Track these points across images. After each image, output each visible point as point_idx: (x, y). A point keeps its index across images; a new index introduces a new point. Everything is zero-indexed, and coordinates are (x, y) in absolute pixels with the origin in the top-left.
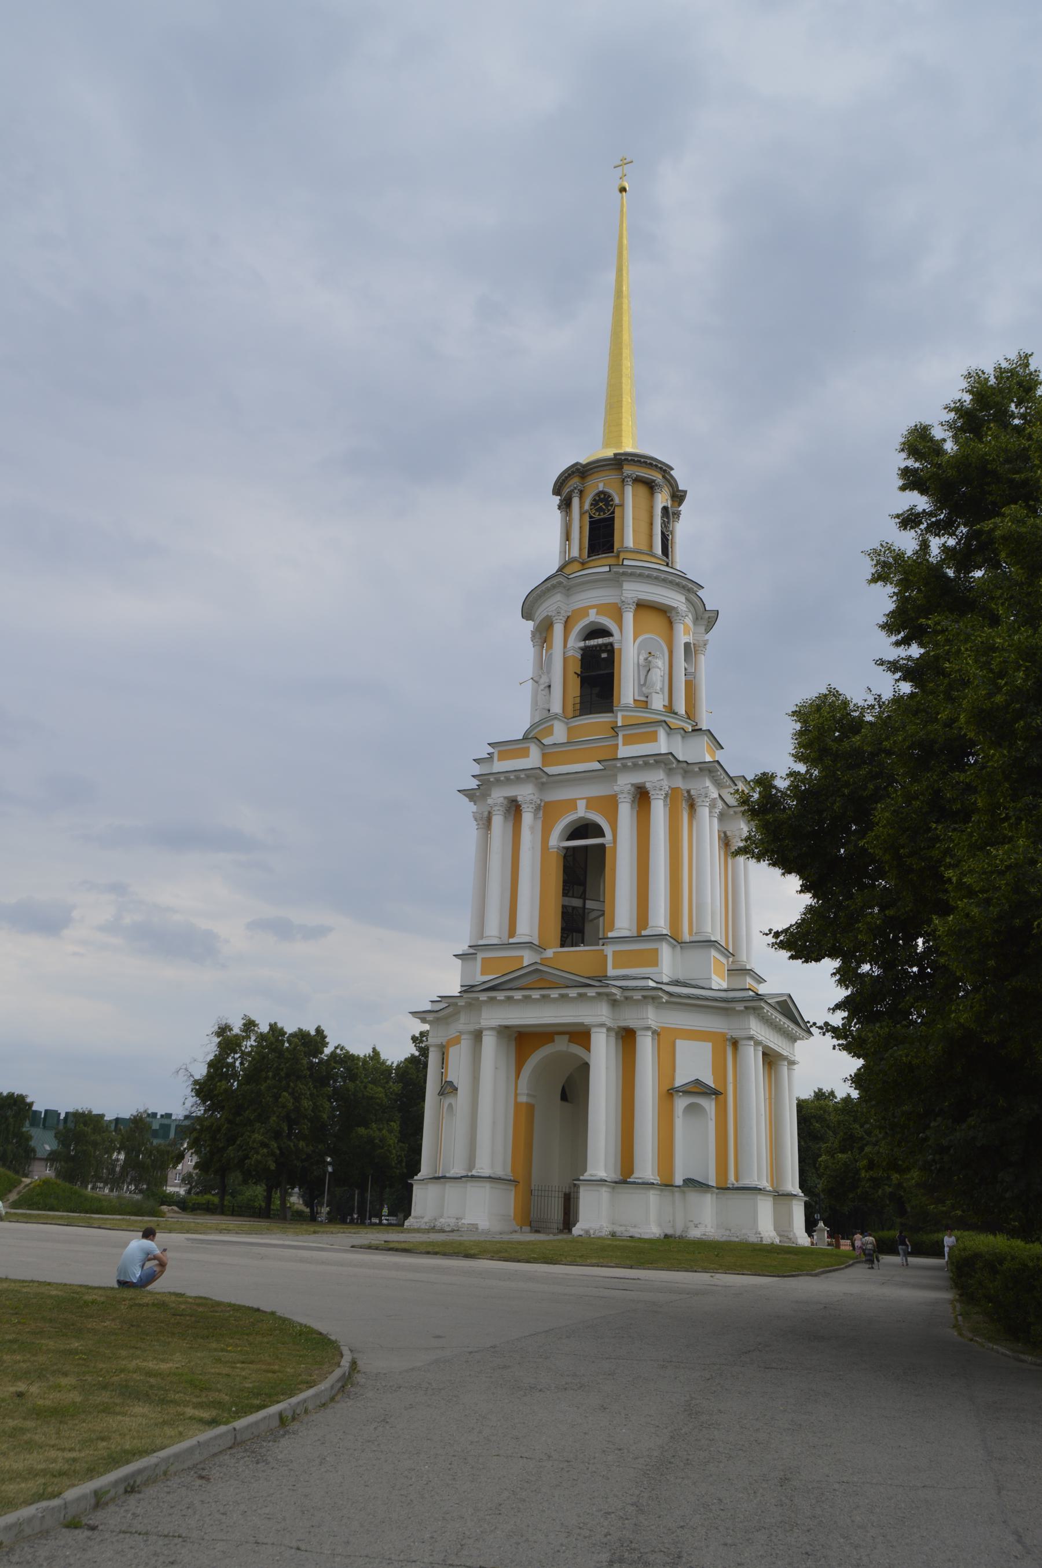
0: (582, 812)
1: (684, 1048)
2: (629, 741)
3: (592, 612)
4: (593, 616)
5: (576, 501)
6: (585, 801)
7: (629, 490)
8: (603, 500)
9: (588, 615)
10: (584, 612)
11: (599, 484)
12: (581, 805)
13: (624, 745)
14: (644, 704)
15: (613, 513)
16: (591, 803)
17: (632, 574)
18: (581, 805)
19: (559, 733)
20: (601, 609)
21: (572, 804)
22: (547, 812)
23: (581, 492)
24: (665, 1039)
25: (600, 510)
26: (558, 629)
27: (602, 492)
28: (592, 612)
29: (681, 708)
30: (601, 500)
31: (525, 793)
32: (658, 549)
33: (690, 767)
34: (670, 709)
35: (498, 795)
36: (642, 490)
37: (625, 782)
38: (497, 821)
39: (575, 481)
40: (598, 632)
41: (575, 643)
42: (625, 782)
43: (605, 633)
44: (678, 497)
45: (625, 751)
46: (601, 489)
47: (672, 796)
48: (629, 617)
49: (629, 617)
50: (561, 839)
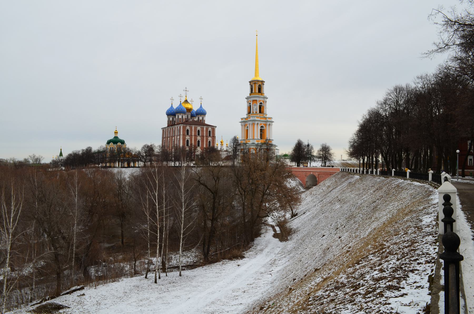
0: (262, 125)
4: (261, 102)
5: (257, 84)
11: (260, 83)
16: (263, 124)
39: (257, 82)
40: (261, 103)
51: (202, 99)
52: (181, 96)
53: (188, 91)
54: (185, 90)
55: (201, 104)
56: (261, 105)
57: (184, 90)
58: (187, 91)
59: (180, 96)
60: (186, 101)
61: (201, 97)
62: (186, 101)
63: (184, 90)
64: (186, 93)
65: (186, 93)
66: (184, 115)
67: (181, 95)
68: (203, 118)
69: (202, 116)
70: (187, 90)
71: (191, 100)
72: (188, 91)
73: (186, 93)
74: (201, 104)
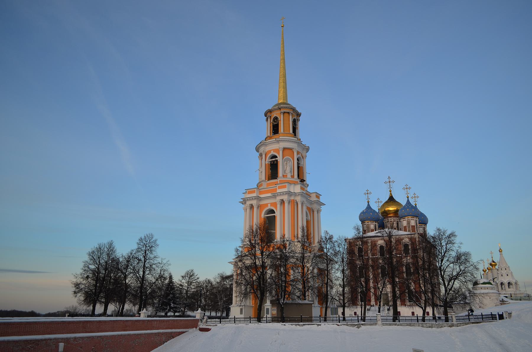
0: (269, 207)
2: (280, 188)
4: (272, 153)
5: (269, 119)
6: (270, 204)
8: (276, 118)
10: (270, 151)
11: (274, 115)
12: (269, 205)
13: (279, 189)
15: (278, 122)
17: (281, 141)
18: (269, 205)
19: (264, 185)
21: (267, 205)
22: (259, 207)
23: (270, 117)
25: (275, 121)
26: (264, 156)
27: (275, 117)
28: (272, 151)
30: (276, 119)
31: (254, 202)
32: (291, 131)
33: (296, 194)
35: (248, 203)
36: (286, 115)
37: (279, 198)
38: (248, 210)
41: (268, 160)
42: (279, 198)
43: (276, 157)
44: (299, 115)
45: (279, 191)
48: (281, 152)
50: (265, 214)
51: (410, 188)
52: (369, 192)
53: (393, 182)
54: (388, 180)
55: (408, 198)
56: (273, 161)
57: (386, 183)
58: (391, 183)
59: (366, 192)
60: (391, 200)
61: (406, 185)
62: (391, 200)
63: (386, 183)
64: (390, 186)
65: (390, 186)
66: (370, 223)
67: (367, 190)
68: (409, 223)
69: (406, 219)
70: (391, 180)
71: (413, 196)
72: (393, 182)
73: (390, 184)
74: (408, 198)
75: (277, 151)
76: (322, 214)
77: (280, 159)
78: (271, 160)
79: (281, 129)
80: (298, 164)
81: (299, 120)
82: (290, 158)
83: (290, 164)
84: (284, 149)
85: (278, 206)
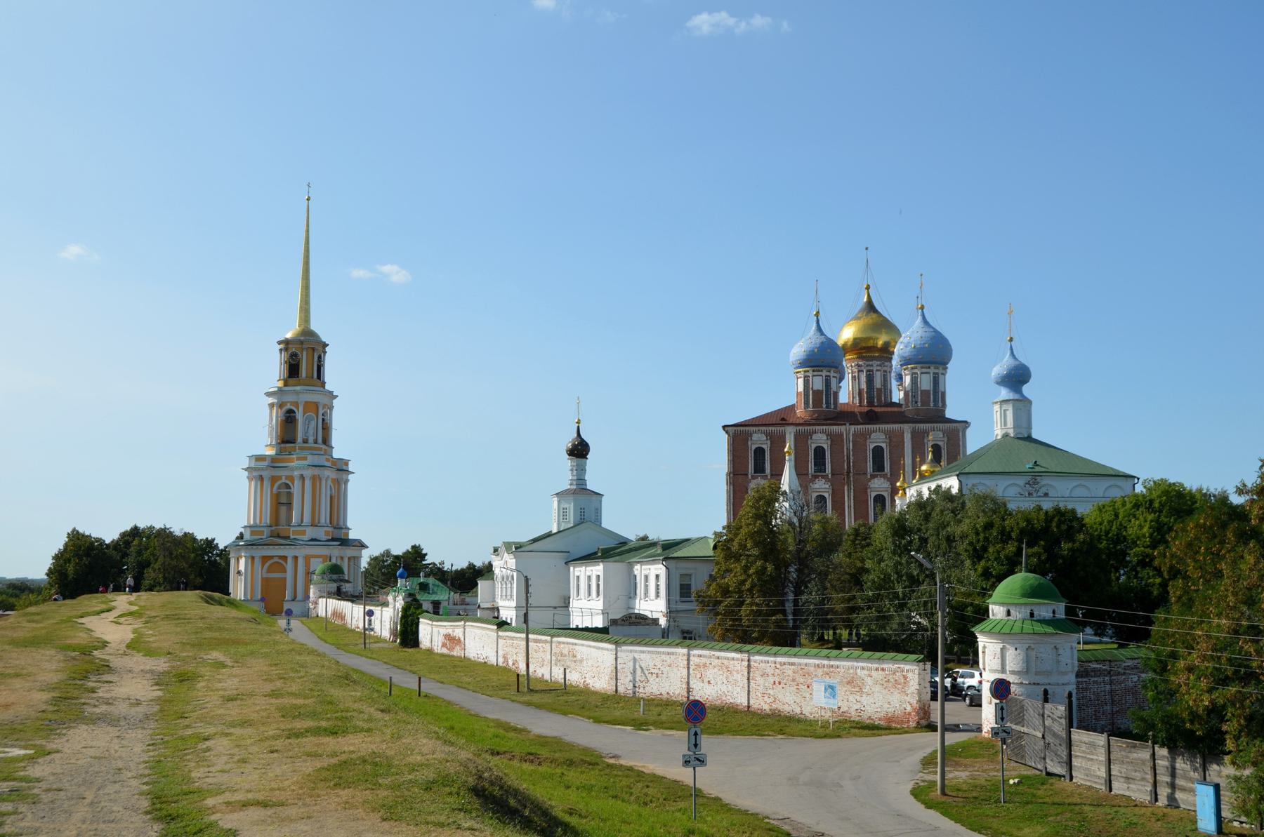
0: (284, 480)
1: (312, 560)
3: (289, 404)
4: (289, 406)
7: (305, 353)
9: (287, 405)
12: (284, 477)
14: (305, 441)
18: (284, 477)
20: (292, 403)
21: (280, 478)
24: (307, 559)
28: (289, 404)
29: (320, 440)
31: (265, 474)
34: (316, 442)
40: (290, 411)
43: (293, 411)
46: (294, 350)
47: (314, 478)
48: (301, 408)
49: (301, 408)
75: (297, 404)
76: (350, 485)
77: (300, 416)
78: (288, 415)
79: (303, 372)
80: (323, 420)
81: (325, 352)
82: (310, 414)
83: (313, 424)
84: (306, 403)
85: (296, 482)
